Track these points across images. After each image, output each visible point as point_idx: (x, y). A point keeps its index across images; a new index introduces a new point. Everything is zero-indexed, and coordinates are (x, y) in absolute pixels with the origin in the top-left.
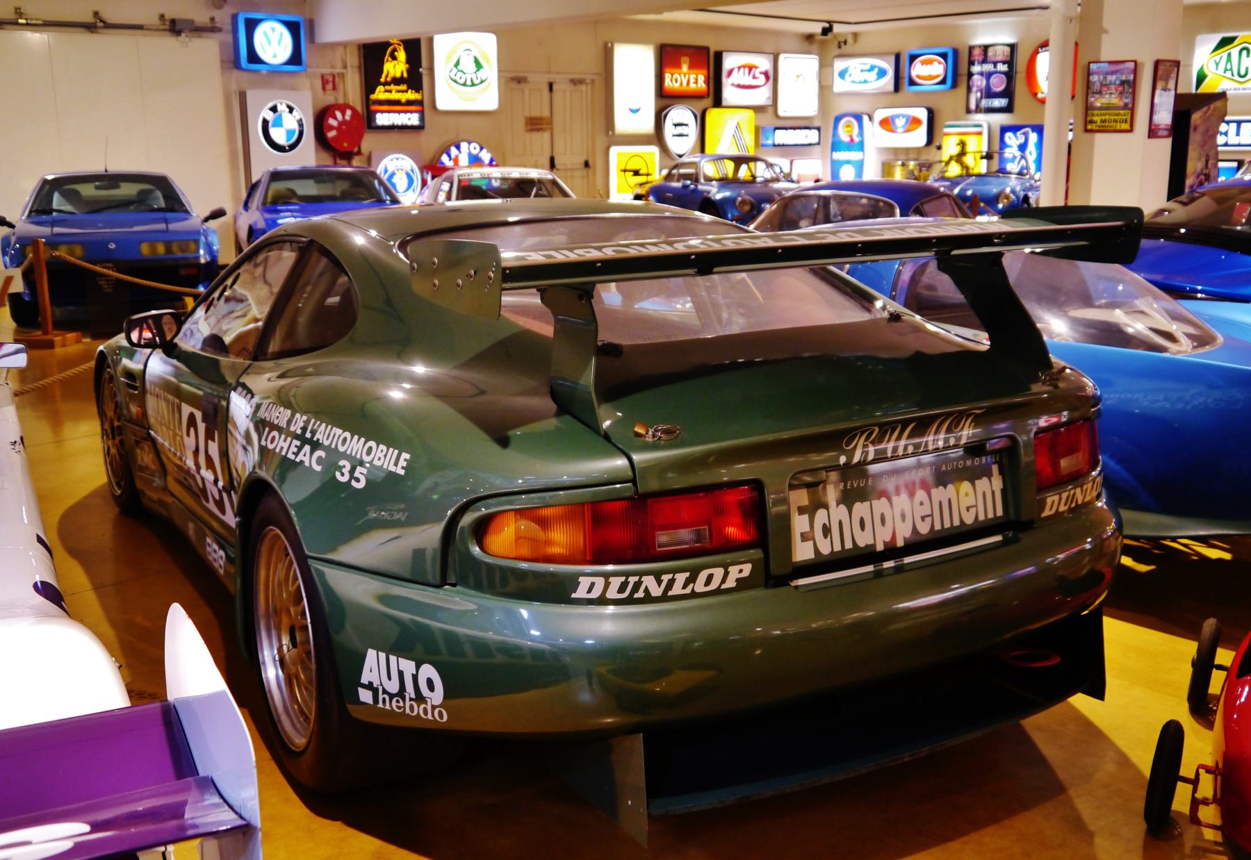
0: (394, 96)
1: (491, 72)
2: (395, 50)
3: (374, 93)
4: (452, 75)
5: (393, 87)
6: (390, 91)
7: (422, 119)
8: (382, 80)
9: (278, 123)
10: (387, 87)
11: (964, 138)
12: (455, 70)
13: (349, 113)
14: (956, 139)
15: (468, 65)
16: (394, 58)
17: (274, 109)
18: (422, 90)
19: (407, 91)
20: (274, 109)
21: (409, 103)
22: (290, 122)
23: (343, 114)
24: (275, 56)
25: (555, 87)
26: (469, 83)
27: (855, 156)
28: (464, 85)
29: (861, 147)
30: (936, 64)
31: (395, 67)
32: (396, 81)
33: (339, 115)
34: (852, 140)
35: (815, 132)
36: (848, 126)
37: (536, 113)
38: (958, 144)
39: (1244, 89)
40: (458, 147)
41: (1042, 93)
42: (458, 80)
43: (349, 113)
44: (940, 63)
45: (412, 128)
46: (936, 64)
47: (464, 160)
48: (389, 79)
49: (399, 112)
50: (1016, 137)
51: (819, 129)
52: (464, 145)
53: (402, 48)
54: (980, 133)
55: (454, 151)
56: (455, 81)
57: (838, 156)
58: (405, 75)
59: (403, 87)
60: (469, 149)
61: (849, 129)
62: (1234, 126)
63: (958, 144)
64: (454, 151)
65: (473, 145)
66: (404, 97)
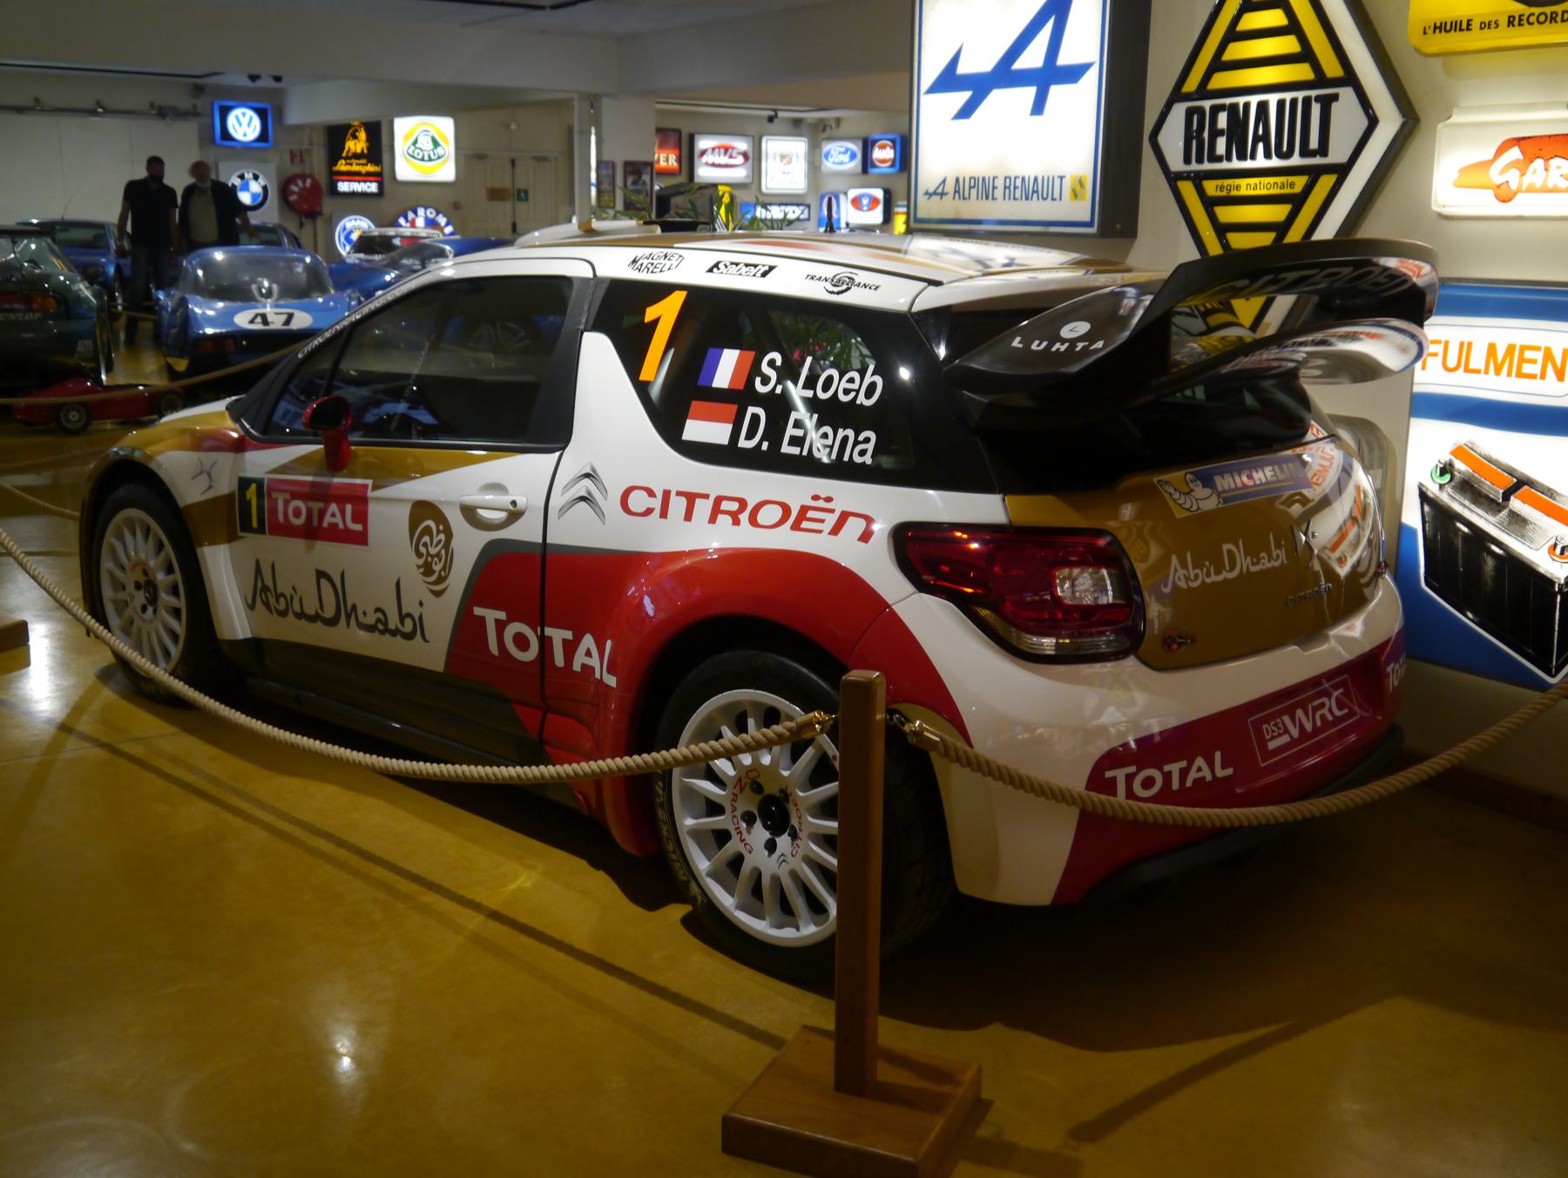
0: (355, 168)
1: (449, 147)
2: (356, 131)
3: (336, 165)
4: (410, 152)
5: (353, 161)
6: (351, 164)
7: (381, 187)
8: (344, 155)
9: (246, 188)
10: (348, 161)
12: (413, 148)
13: (309, 181)
15: (425, 143)
16: (355, 137)
17: (242, 177)
18: (382, 163)
19: (366, 165)
20: (242, 177)
21: (369, 174)
22: (255, 187)
23: (304, 183)
24: (245, 135)
25: (517, 163)
26: (426, 158)
28: (422, 160)
30: (888, 148)
31: (357, 145)
32: (356, 156)
33: (300, 183)
37: (498, 185)
40: (415, 213)
42: (416, 155)
43: (309, 181)
44: (891, 148)
45: (371, 195)
46: (888, 148)
47: (420, 222)
48: (350, 155)
49: (359, 181)
52: (421, 211)
53: (362, 129)
55: (411, 215)
56: (414, 157)
58: (365, 151)
59: (364, 161)
60: (425, 213)
64: (411, 215)
65: (429, 211)
66: (364, 169)
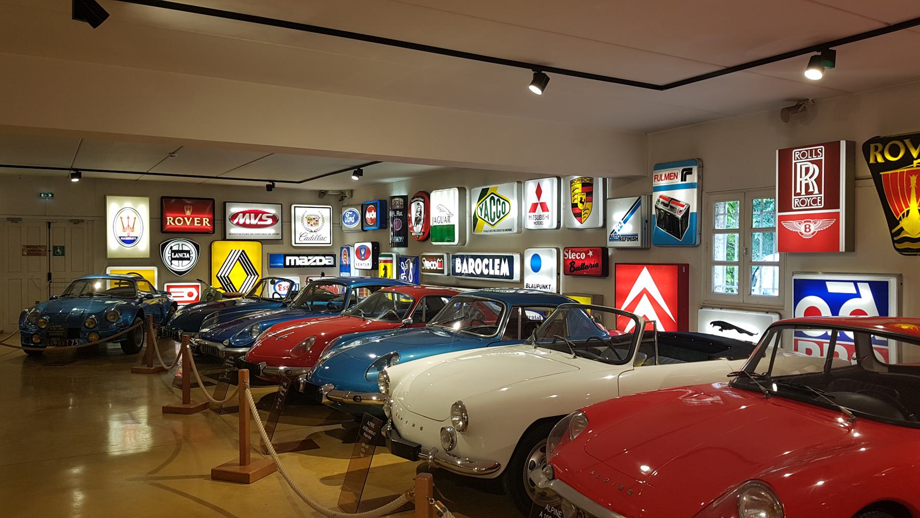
34: (347, 265)
36: (345, 255)
39: (494, 231)
50: (405, 265)
51: (334, 256)
54: (391, 261)
62: (491, 260)
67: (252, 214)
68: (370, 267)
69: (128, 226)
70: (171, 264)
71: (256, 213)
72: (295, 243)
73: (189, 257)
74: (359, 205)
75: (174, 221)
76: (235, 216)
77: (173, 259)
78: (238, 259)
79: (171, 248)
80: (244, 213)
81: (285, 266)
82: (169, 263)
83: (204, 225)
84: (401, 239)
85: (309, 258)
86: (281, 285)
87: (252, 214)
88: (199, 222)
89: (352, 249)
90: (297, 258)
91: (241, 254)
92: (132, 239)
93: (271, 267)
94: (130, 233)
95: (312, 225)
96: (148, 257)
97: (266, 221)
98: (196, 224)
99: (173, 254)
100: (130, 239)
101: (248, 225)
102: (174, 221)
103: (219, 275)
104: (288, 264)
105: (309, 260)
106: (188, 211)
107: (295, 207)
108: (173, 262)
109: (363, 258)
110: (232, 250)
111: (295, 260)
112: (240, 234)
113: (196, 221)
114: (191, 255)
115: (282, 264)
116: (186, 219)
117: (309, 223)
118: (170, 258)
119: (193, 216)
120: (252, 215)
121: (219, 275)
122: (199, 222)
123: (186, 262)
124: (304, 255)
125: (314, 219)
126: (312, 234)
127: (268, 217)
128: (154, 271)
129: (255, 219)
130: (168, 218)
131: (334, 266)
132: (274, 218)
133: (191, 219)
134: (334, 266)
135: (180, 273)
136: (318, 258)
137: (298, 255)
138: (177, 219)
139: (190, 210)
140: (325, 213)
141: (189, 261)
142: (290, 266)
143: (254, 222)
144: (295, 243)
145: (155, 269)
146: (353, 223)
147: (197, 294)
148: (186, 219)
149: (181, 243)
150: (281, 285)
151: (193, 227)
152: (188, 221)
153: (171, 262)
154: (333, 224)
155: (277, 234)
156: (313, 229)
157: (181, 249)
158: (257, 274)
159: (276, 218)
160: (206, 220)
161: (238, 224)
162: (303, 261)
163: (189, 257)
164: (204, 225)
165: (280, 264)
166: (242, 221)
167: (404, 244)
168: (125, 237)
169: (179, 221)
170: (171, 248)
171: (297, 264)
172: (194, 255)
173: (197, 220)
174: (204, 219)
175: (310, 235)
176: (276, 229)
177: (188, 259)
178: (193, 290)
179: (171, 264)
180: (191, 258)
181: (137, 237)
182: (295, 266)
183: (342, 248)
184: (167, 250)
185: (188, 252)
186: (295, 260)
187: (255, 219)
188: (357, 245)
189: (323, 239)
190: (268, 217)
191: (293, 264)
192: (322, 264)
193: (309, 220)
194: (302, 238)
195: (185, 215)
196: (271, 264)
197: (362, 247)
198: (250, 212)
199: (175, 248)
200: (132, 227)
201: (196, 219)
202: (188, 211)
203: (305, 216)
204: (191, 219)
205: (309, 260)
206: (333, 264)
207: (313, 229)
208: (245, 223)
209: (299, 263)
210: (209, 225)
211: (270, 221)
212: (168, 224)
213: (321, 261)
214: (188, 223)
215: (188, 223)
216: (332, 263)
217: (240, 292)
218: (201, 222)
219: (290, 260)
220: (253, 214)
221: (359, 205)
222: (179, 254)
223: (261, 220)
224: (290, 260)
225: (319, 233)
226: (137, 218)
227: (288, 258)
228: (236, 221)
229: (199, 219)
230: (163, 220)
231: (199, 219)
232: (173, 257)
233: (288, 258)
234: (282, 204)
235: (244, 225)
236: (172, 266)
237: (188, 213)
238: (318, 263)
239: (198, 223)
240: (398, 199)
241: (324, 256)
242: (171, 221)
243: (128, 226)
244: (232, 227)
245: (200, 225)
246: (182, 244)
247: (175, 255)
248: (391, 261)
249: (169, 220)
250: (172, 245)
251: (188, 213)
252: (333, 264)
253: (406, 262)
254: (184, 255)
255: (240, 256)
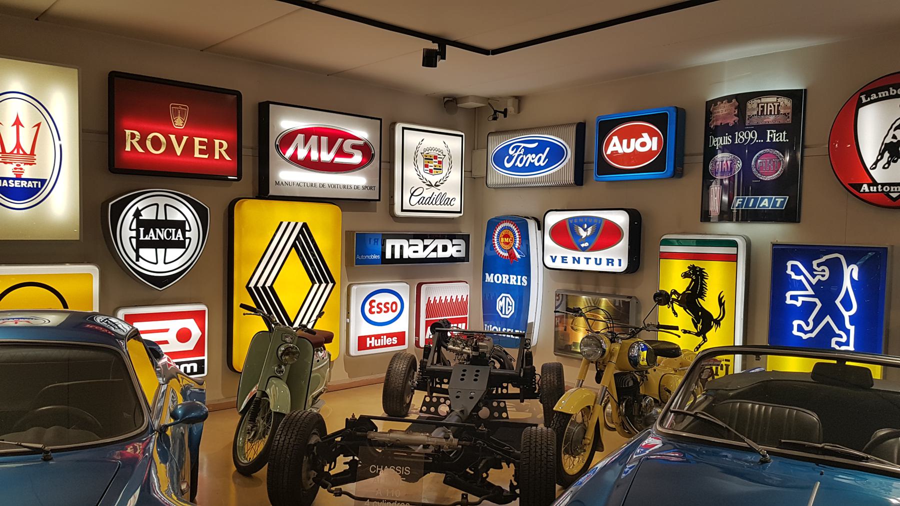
11: (698, 264)
14: (681, 266)
27: (514, 280)
29: (524, 268)
34: (512, 255)
35: (462, 242)
36: (506, 236)
38: (685, 275)
41: (875, 184)
50: (811, 270)
51: (466, 238)
54: (733, 258)
57: (490, 278)
61: (507, 240)
63: (685, 275)
67: (322, 138)
68: (620, 266)
69: (18, 146)
70: (138, 257)
71: (333, 137)
72: (403, 210)
73: (182, 239)
74: (569, 125)
75: (142, 143)
76: (288, 138)
77: (141, 244)
78: (294, 245)
79: (138, 214)
80: (307, 133)
81: (384, 261)
82: (133, 255)
83: (217, 157)
84: (779, 200)
85: (427, 242)
86: (374, 301)
87: (322, 138)
88: (204, 147)
89: (532, 226)
90: (404, 242)
91: (301, 232)
92: (30, 185)
93: (359, 262)
94: (22, 166)
95: (431, 171)
96: (78, 239)
97: (350, 156)
98: (197, 155)
99: (142, 230)
100: (24, 184)
101: (314, 162)
102: (142, 143)
103: (252, 285)
104: (388, 255)
105: (425, 247)
106: (179, 117)
107: (404, 128)
108: (143, 252)
109: (583, 245)
110: (281, 223)
111: (402, 247)
112: (299, 185)
113: (197, 147)
114: (188, 234)
115: (379, 257)
116: (173, 137)
117: (426, 166)
118: (134, 241)
119: (192, 131)
120: (324, 139)
121: (252, 285)
122: (204, 147)
123: (173, 253)
124: (416, 237)
125: (436, 157)
126: (433, 189)
127: (354, 147)
128: (90, 276)
129: (329, 151)
130: (128, 132)
131: (465, 259)
132: (365, 149)
133: (185, 138)
134: (465, 259)
135: (161, 281)
136: (440, 243)
137: (407, 237)
138: (150, 136)
139: (182, 115)
140: (454, 144)
141: (182, 250)
142: (393, 260)
143: (326, 157)
144: (403, 210)
145: (93, 270)
146: (540, 168)
147: (200, 334)
148: (173, 137)
149: (162, 201)
150: (374, 301)
151: (188, 160)
152: (179, 146)
153: (137, 251)
154: (464, 171)
155: (371, 188)
156: (433, 179)
157: (161, 217)
158: (333, 281)
159: (371, 151)
160: (221, 146)
161: (294, 159)
162: (415, 248)
163: (182, 239)
164: (217, 157)
165: (375, 257)
166: (302, 154)
167: (789, 215)
168: (8, 179)
169: (156, 143)
170: (138, 214)
171: (405, 256)
172: (193, 234)
173: (201, 143)
174: (217, 142)
175: (427, 194)
176: (368, 176)
177: (180, 244)
178: (190, 324)
179: (138, 257)
180: (187, 241)
181: (43, 181)
182: (402, 260)
183: (492, 224)
184: (127, 218)
185: (180, 225)
186: (402, 247)
187: (329, 151)
188: (553, 219)
189: (449, 201)
190: (354, 147)
191: (397, 256)
192: (446, 255)
193: (428, 159)
194: (415, 200)
195: (172, 129)
196: (358, 257)
197: (580, 220)
198: (319, 132)
199: (147, 215)
200: (28, 151)
201: (197, 140)
202: (179, 117)
203: (421, 150)
204: (185, 138)
205: (425, 247)
206: (464, 255)
207: (433, 179)
208: (308, 156)
209: (408, 253)
210: (228, 158)
211: (357, 158)
212: (128, 149)
213: (445, 248)
214: (179, 151)
215: (179, 151)
216: (462, 254)
217: (296, 325)
218: (210, 149)
219: (393, 247)
220: (326, 138)
221: (569, 125)
222: (158, 230)
223: (340, 153)
224: (393, 247)
225: (443, 189)
226: (44, 125)
227: (389, 243)
228: (290, 152)
229: (206, 140)
230: (114, 139)
231: (206, 140)
232: (142, 238)
233: (389, 243)
234: (381, 120)
235: (308, 164)
236: (141, 263)
237: (179, 123)
238: (441, 254)
239: (201, 152)
240: (774, 99)
241: (451, 237)
242: (134, 142)
243: (18, 146)
244: (280, 167)
245: (206, 156)
246: (166, 205)
247: (146, 233)
248: (733, 258)
249: (131, 140)
250: (140, 206)
251: (179, 123)
252: (464, 255)
253: (815, 263)
254: (169, 234)
255: (297, 238)
